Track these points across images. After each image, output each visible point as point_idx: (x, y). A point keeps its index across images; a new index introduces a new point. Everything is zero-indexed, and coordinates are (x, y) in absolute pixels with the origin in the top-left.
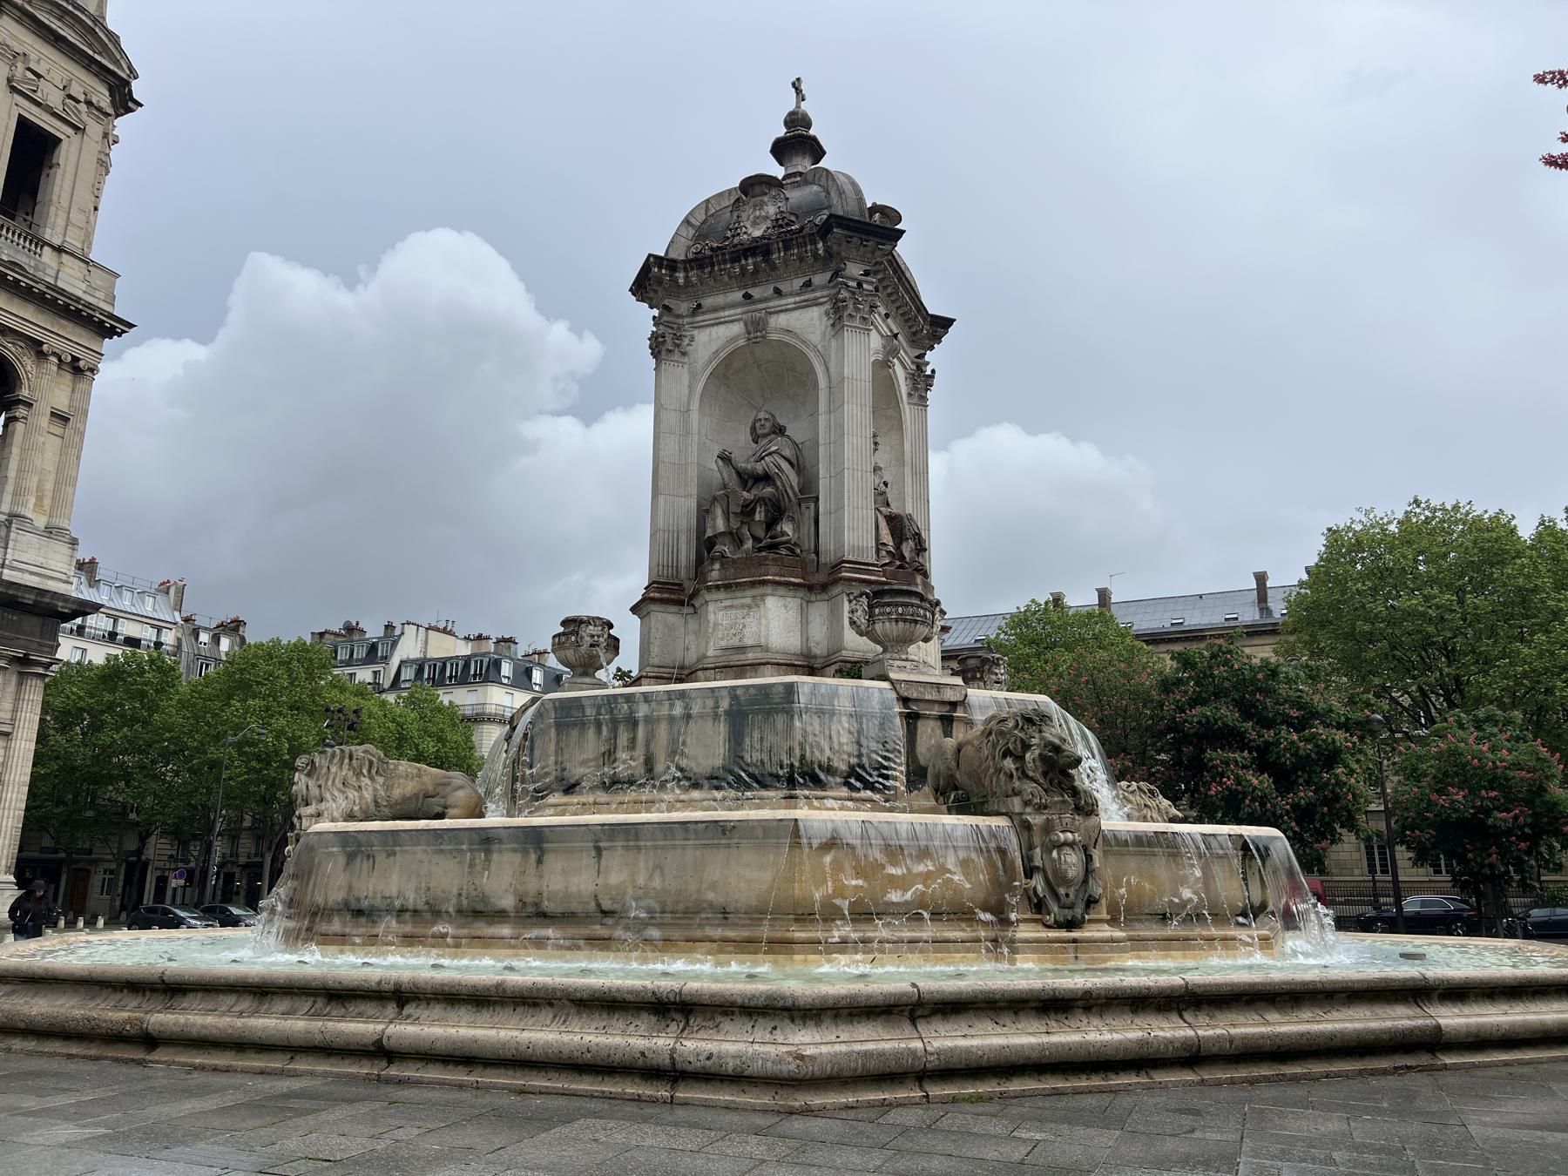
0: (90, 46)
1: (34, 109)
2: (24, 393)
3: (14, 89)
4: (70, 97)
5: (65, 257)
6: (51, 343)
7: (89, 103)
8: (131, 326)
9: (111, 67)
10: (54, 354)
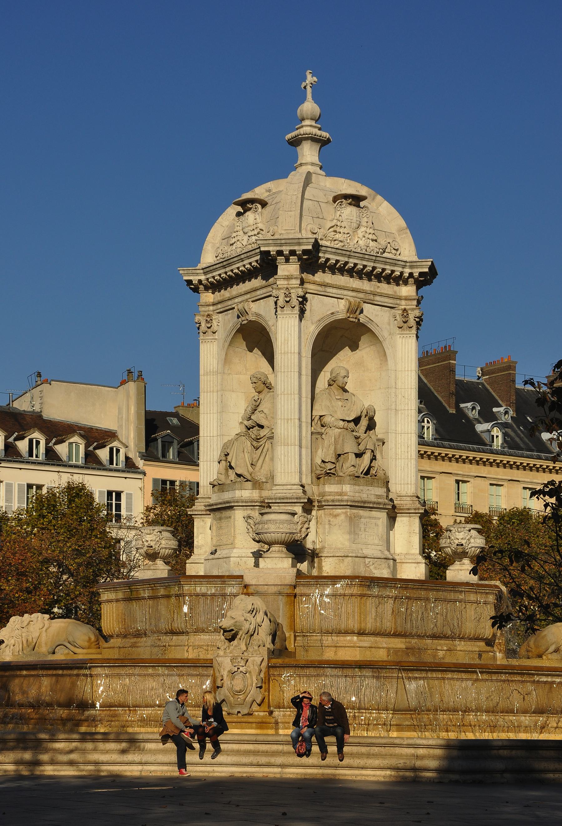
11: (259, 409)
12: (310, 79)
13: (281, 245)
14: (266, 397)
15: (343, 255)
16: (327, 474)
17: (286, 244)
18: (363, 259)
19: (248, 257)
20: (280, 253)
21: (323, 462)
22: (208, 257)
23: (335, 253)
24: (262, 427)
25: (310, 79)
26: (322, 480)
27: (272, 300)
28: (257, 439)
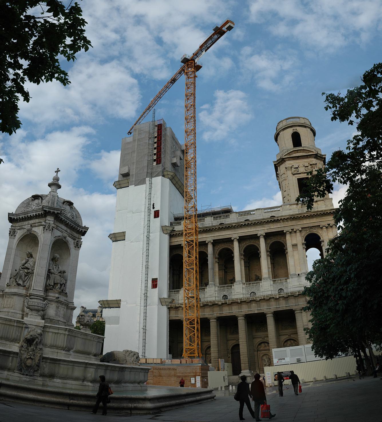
1: (300, 175)
3: (294, 174)
4: (306, 167)
6: (322, 224)
9: (311, 154)
10: (323, 226)
13: (50, 209)
14: (31, 260)
15: (66, 219)
16: (50, 289)
17: (52, 209)
18: (71, 222)
19: (36, 212)
21: (49, 285)
23: (64, 217)
24: (29, 269)
27: (41, 227)
28: (27, 273)
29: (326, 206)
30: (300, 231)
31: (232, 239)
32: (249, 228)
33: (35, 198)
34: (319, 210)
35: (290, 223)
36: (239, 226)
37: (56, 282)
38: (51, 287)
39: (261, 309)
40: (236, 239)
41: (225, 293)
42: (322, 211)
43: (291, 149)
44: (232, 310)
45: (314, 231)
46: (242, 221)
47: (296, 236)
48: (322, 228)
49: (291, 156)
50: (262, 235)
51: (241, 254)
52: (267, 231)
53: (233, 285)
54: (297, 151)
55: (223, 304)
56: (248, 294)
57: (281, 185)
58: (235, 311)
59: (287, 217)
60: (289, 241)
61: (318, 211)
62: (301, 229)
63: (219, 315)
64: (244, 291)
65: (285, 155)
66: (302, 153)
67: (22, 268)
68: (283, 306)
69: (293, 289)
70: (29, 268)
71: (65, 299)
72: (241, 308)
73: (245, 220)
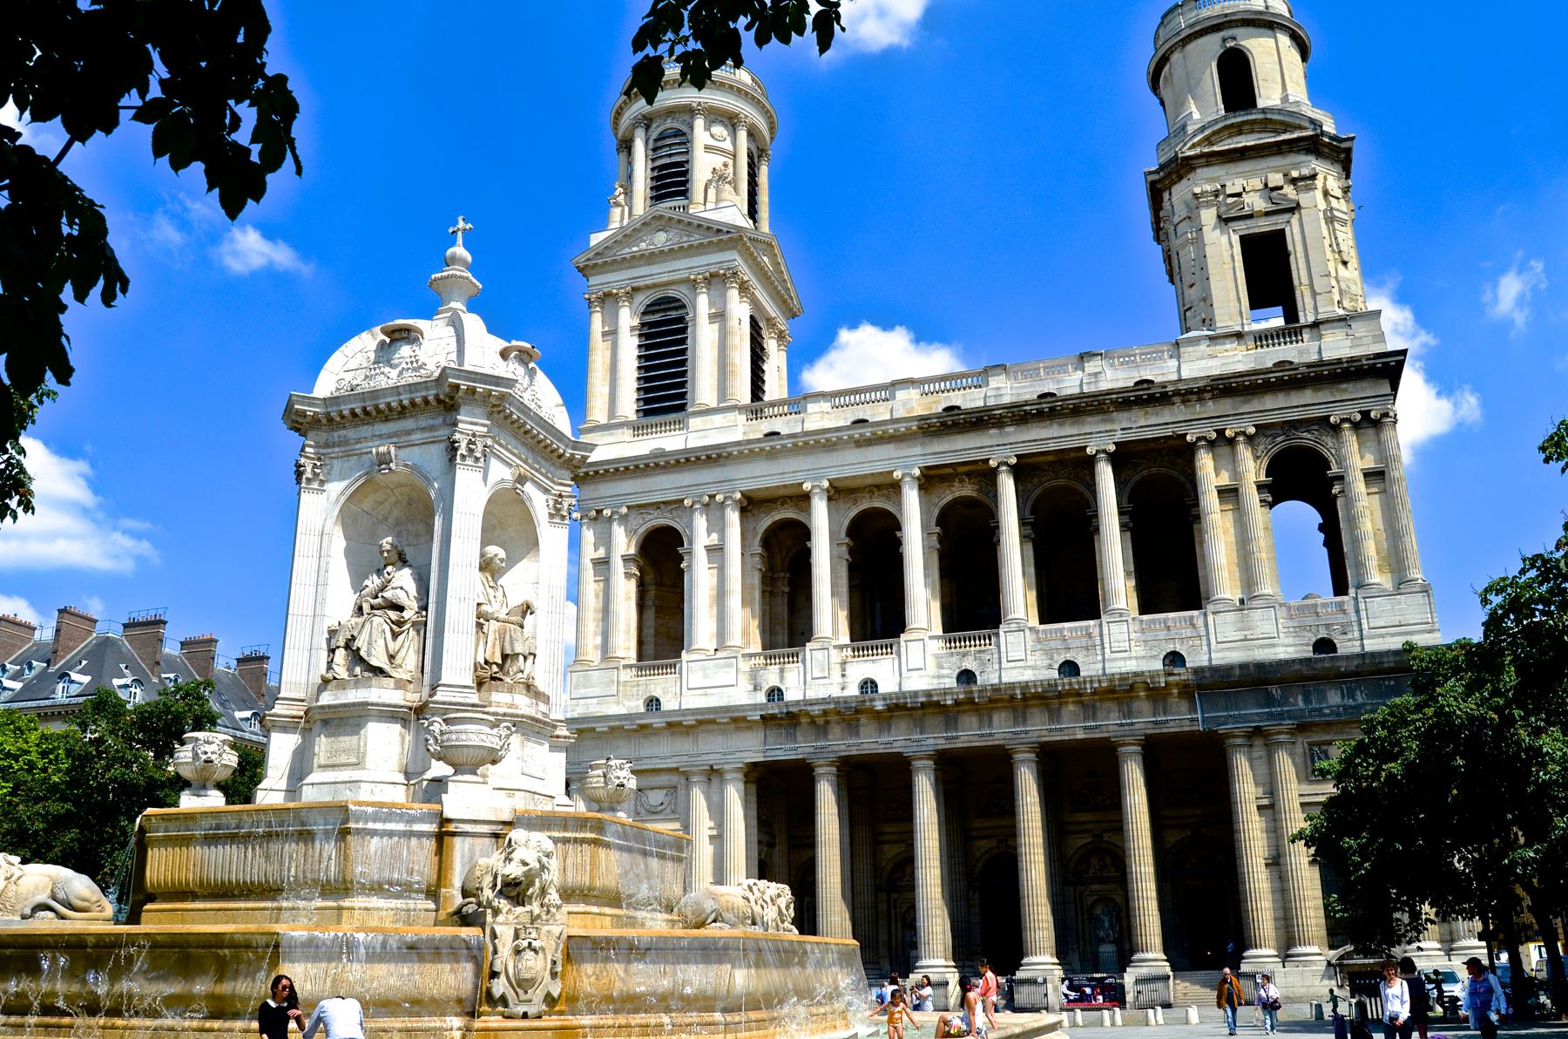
0: (1279, 133)
1: (1249, 222)
2: (1335, 469)
4: (1273, 189)
5: (1324, 330)
7: (1294, 181)
8: (1404, 352)
9: (1295, 136)
10: (1343, 420)
11: (392, 584)
12: (461, 224)
16: (493, 679)
20: (472, 391)
21: (486, 662)
22: (325, 386)
24: (401, 609)
25: (461, 224)
26: (485, 687)
28: (400, 623)
29: (1357, 341)
30: (1250, 439)
31: (993, 463)
32: (1055, 426)
33: (397, 335)
34: (1327, 356)
35: (1212, 408)
36: (1019, 415)
37: (508, 651)
38: (495, 668)
39: (1096, 727)
40: (1006, 464)
41: (969, 664)
42: (1339, 361)
43: (1216, 121)
44: (990, 726)
45: (1307, 438)
46: (1027, 397)
47: (1234, 454)
48: (1336, 429)
49: (1215, 148)
50: (1104, 451)
51: (1022, 522)
52: (1119, 436)
53: (997, 635)
54: (1239, 129)
55: (957, 703)
56: (1050, 667)
57: (1175, 263)
58: (1000, 730)
59: (1202, 384)
60: (1209, 472)
61: (1321, 363)
62: (1252, 430)
63: (942, 744)
64: (1038, 659)
65: (1193, 146)
66: (1257, 136)
67: (372, 608)
68: (1182, 719)
69: (1220, 655)
70: (402, 599)
71: (543, 707)
72: (1025, 719)
73: (1040, 397)
